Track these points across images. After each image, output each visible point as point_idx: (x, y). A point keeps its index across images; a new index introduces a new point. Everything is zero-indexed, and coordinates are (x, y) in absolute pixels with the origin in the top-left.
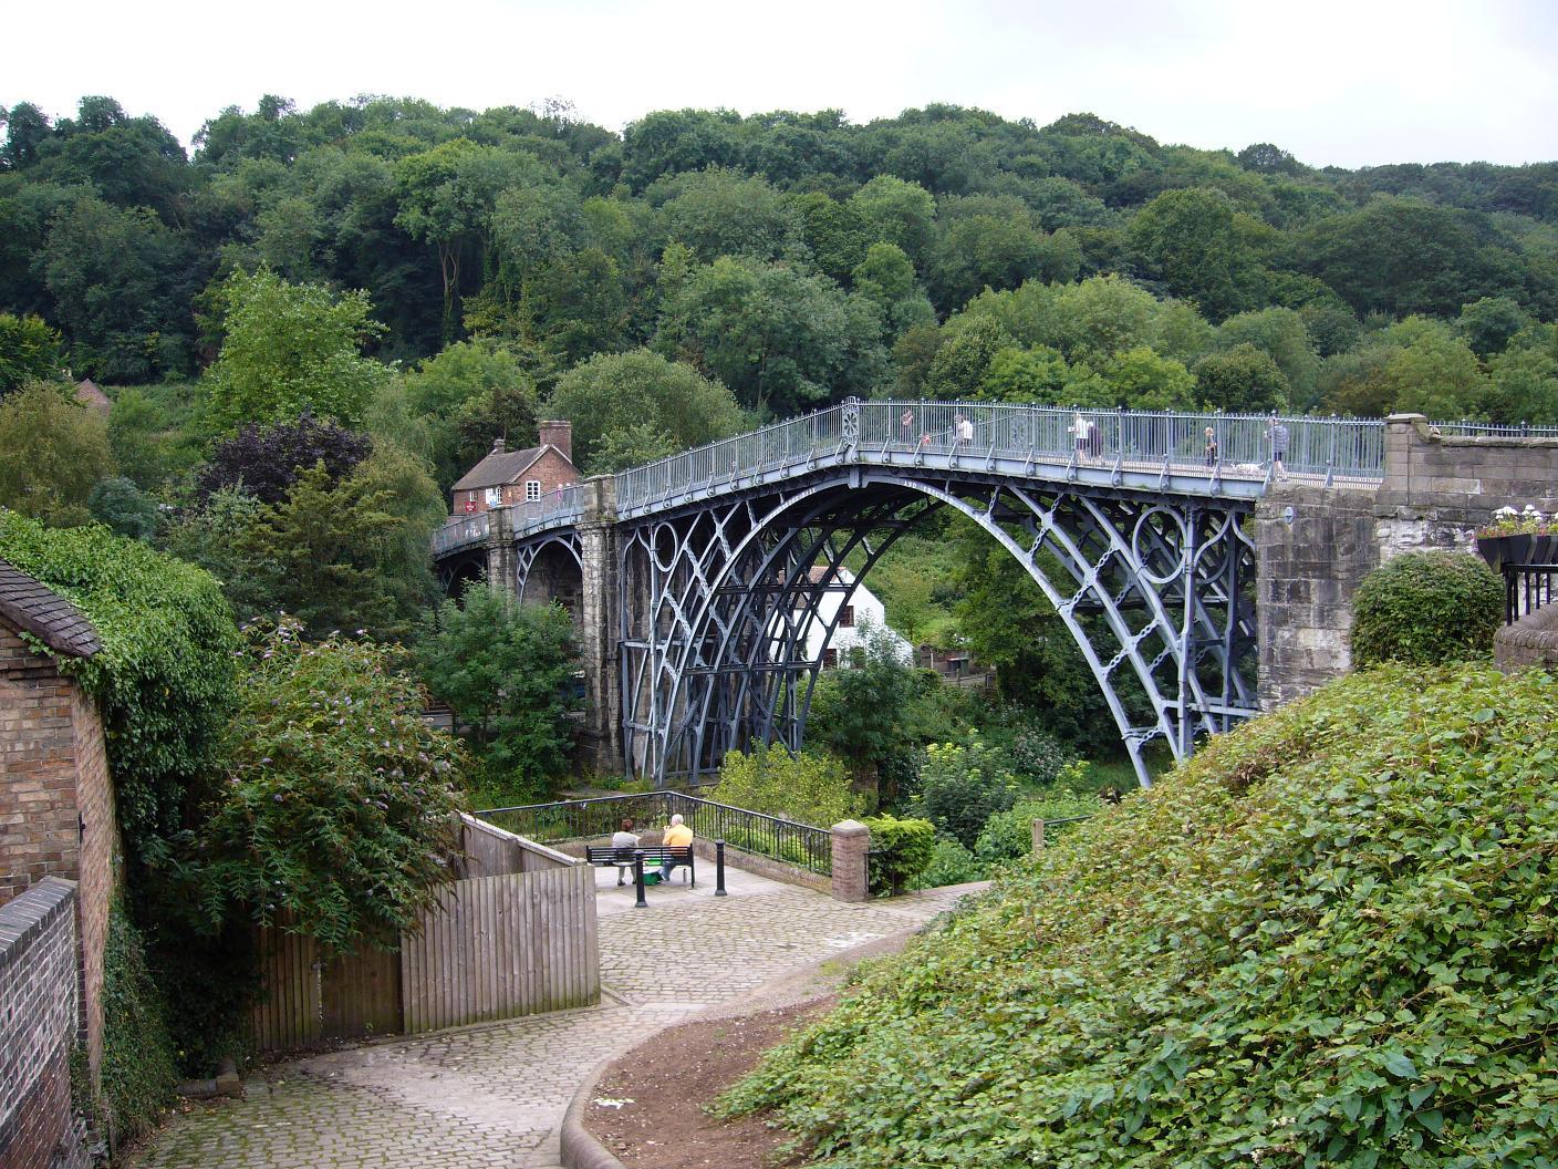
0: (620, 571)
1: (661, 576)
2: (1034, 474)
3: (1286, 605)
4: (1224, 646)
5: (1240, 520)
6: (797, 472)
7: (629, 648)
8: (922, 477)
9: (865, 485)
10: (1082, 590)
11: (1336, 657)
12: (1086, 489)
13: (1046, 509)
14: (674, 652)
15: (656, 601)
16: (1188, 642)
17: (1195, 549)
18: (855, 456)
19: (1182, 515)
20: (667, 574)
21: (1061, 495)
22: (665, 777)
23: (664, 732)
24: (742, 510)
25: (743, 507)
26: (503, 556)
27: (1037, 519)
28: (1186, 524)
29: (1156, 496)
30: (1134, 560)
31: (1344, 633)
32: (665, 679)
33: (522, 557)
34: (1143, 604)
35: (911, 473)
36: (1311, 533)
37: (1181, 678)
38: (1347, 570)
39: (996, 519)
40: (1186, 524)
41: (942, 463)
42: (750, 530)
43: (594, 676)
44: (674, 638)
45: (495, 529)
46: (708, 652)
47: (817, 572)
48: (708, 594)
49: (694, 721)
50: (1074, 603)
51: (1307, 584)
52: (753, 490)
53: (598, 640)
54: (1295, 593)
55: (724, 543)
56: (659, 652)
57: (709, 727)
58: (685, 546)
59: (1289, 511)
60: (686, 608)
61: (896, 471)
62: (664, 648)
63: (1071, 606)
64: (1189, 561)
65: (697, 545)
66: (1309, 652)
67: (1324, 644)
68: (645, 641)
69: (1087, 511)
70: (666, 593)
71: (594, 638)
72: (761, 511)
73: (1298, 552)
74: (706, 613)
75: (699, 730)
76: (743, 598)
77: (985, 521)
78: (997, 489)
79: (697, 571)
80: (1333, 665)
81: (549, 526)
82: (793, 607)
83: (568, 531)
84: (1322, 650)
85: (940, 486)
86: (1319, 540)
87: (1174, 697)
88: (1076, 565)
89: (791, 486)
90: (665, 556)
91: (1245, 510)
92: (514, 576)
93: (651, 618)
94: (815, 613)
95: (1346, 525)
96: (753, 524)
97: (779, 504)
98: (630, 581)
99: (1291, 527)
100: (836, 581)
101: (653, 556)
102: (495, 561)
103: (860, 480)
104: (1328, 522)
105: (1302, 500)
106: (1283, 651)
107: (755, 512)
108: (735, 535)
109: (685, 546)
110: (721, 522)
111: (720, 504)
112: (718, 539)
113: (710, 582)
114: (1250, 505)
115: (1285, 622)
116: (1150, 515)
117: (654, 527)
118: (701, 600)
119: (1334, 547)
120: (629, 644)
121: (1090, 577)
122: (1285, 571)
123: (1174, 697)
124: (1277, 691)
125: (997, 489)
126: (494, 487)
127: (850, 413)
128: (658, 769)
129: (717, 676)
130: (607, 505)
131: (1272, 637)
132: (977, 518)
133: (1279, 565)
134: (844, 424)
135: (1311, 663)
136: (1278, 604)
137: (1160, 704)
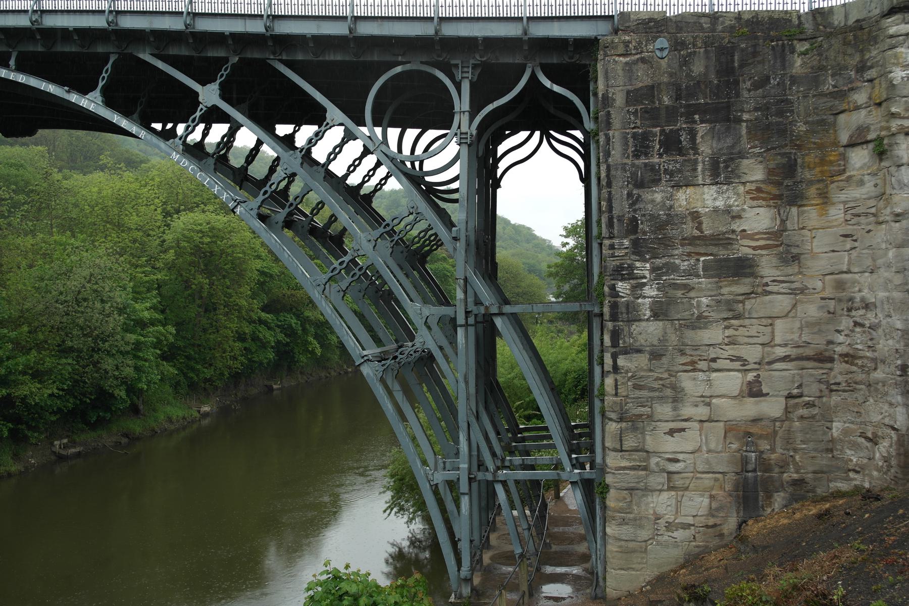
3: (656, 160)
11: (740, 217)
31: (749, 187)
38: (756, 109)
51: (693, 134)
54: (671, 144)
66: (695, 216)
67: (720, 203)
80: (734, 226)
84: (716, 210)
106: (653, 217)
115: (656, 181)
119: (737, 83)
124: (644, 269)
131: (634, 201)
132: (74, 98)
133: (646, 111)
135: (699, 228)
136: (643, 160)
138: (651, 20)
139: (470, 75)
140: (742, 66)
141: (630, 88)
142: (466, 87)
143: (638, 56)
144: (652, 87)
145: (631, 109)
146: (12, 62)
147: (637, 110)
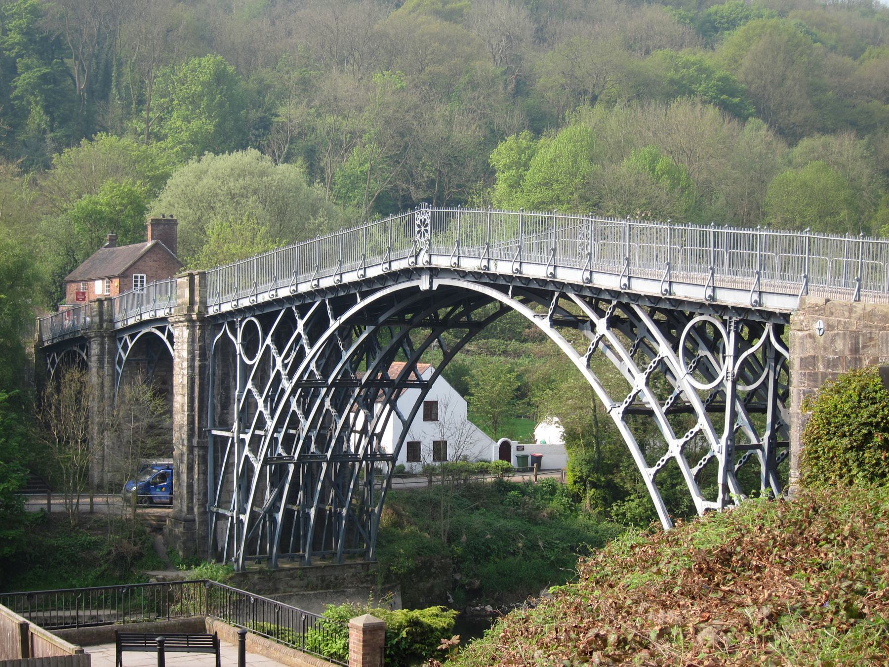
0: (209, 362)
1: (246, 369)
2: (590, 281)
4: (763, 450)
5: (779, 330)
6: (372, 273)
7: (216, 436)
8: (487, 281)
9: (435, 287)
10: (632, 394)
12: (637, 297)
13: (601, 314)
14: (255, 442)
15: (241, 392)
16: (727, 446)
17: (736, 358)
18: (427, 258)
19: (724, 323)
20: (252, 366)
21: (614, 303)
22: (244, 559)
23: (245, 518)
24: (322, 307)
25: (323, 304)
26: (102, 344)
27: (593, 326)
28: (728, 334)
29: (701, 305)
30: (679, 367)
32: (248, 466)
33: (120, 346)
34: (691, 410)
35: (477, 276)
36: (840, 345)
37: (720, 480)
39: (555, 323)
40: (728, 334)
41: (504, 268)
42: (327, 327)
43: (182, 462)
44: (258, 427)
45: (97, 319)
46: (289, 441)
47: (396, 368)
48: (287, 385)
49: (274, 507)
50: (624, 406)
52: (331, 289)
53: (185, 428)
55: (304, 340)
56: (242, 441)
57: (288, 513)
58: (269, 341)
59: (820, 324)
60: (269, 399)
61: (463, 275)
62: (247, 437)
63: (622, 409)
64: (730, 369)
65: (280, 341)
68: (229, 430)
69: (640, 320)
70: (250, 385)
71: (181, 427)
72: (341, 305)
73: (829, 364)
74: (288, 404)
75: (279, 516)
76: (323, 391)
77: (544, 325)
78: (556, 294)
79: (279, 366)
81: (146, 317)
82: (374, 401)
83: (161, 323)
85: (504, 290)
86: (847, 353)
87: (714, 499)
88: (629, 371)
89: (367, 285)
90: (250, 349)
91: (781, 322)
92: (112, 363)
93: (236, 409)
94: (393, 407)
95: (871, 339)
96: (332, 322)
97: (355, 303)
98: (219, 372)
99: (821, 340)
100: (412, 376)
101: (239, 348)
102: (95, 349)
103: (431, 283)
104: (855, 336)
105: (832, 314)
107: (332, 310)
108: (316, 327)
109: (269, 341)
110: (302, 318)
111: (302, 301)
112: (299, 335)
113: (290, 375)
114: (786, 317)
116: (705, 322)
117: (241, 322)
118: (283, 391)
119: (860, 360)
120: (214, 432)
121: (638, 381)
122: (815, 381)
123: (714, 499)
125: (556, 294)
126: (103, 279)
127: (423, 217)
128: (240, 552)
129: (295, 464)
130: (197, 299)
132: (537, 321)
133: (810, 375)
134: (417, 229)
137: (700, 504)
138: (817, 305)
139: (732, 328)
140: (864, 347)
141: (802, 356)
142: (732, 335)
143: (808, 332)
144: (814, 357)
145: (803, 371)
146: (510, 293)
147: (805, 373)
